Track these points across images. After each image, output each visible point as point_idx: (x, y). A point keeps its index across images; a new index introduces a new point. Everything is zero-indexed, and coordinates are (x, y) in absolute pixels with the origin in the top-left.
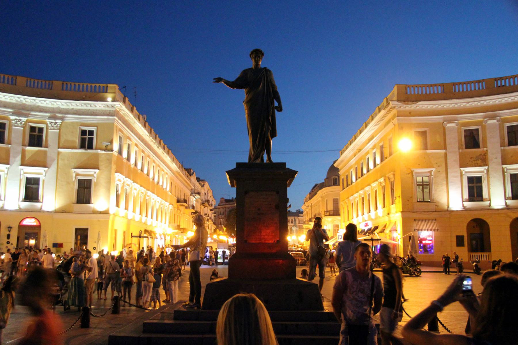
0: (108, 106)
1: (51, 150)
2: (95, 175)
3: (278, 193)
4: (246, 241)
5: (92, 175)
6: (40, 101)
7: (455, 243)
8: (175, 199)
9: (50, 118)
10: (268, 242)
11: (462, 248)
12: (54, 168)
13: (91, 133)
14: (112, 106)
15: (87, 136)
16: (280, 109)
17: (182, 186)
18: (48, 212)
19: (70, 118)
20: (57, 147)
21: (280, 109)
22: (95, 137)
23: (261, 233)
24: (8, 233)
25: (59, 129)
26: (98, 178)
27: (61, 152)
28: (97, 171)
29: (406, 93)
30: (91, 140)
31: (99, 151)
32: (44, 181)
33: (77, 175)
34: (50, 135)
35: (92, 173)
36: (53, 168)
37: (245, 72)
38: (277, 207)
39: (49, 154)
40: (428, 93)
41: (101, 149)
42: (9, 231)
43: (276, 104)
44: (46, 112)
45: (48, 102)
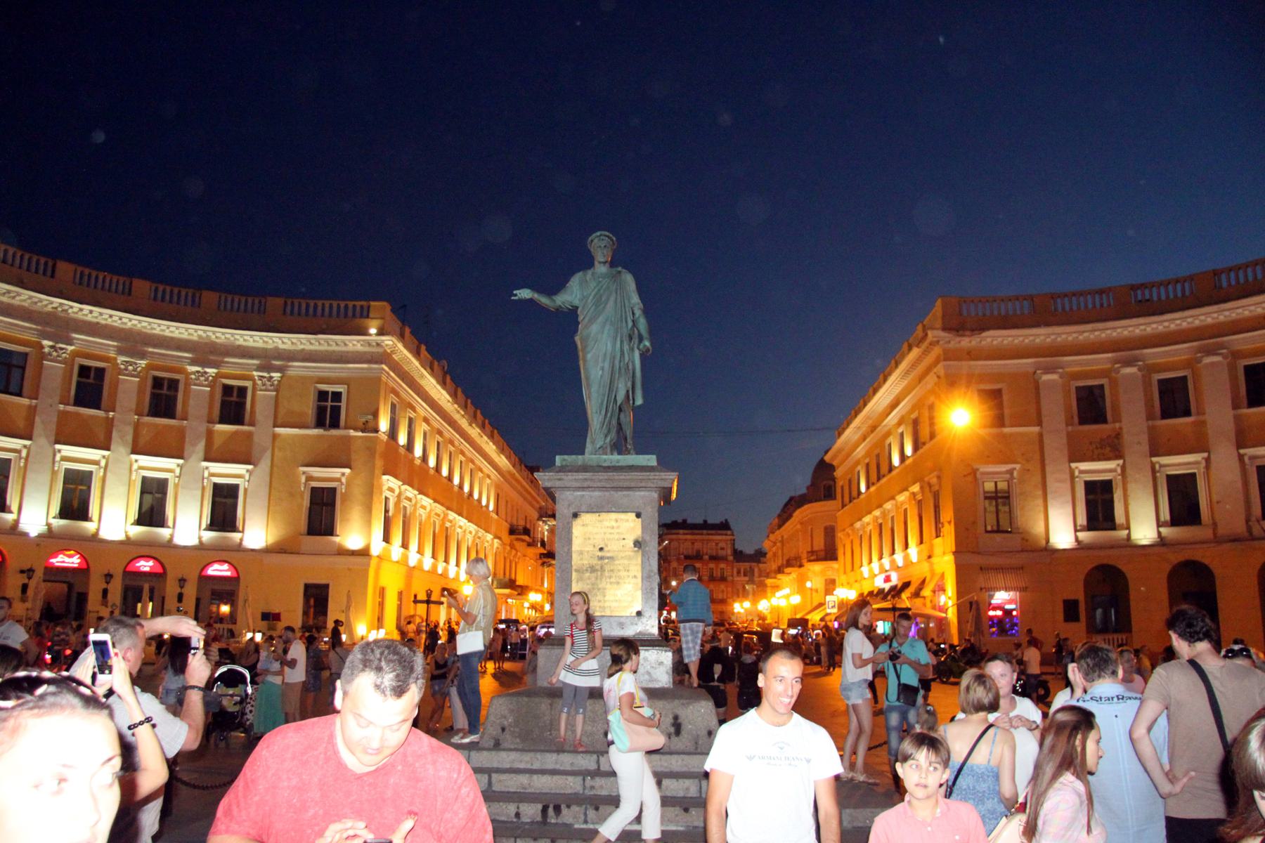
0: (370, 345)
1: (260, 430)
2: (344, 480)
3: (638, 516)
5: (338, 480)
6: (242, 336)
7: (1060, 616)
8: (506, 526)
9: (259, 368)
11: (1072, 626)
12: (265, 464)
13: (337, 396)
14: (378, 345)
15: (329, 404)
17: (520, 500)
18: (253, 550)
19: (298, 369)
20: (271, 423)
22: (343, 405)
24: (104, 586)
25: (277, 390)
26: (348, 485)
27: (279, 435)
28: (347, 471)
30: (336, 411)
31: (352, 433)
32: (246, 490)
33: (310, 478)
34: (260, 402)
35: (338, 475)
36: (265, 464)
39: (256, 439)
41: (355, 429)
42: (108, 583)
44: (252, 357)
45: (257, 338)
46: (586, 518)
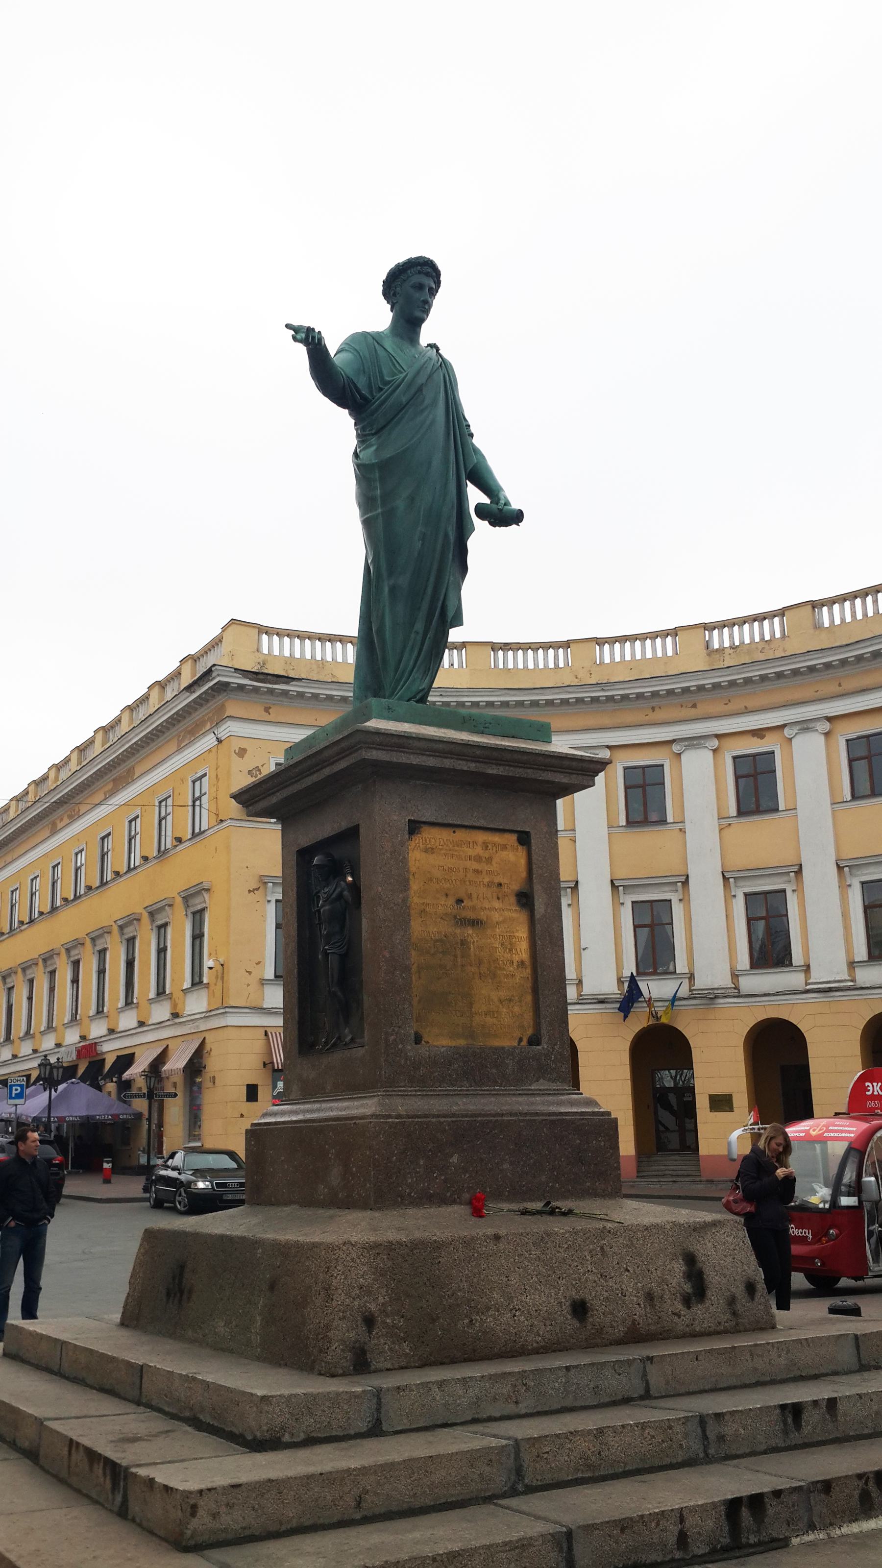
3: (524, 839)
4: (418, 1039)
10: (497, 1043)
16: (503, 516)
21: (503, 516)
23: (471, 1005)
37: (364, 344)
38: (525, 899)
43: (475, 496)
46: (431, 836)
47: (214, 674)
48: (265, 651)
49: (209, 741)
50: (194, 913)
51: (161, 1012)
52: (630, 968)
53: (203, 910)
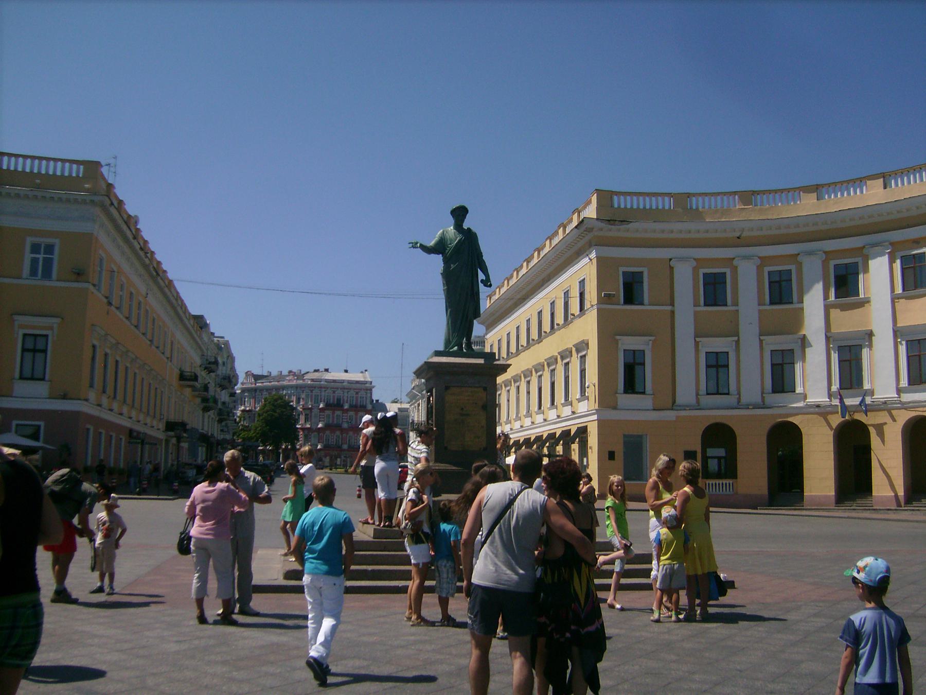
3: (485, 389)
4: (446, 448)
16: (487, 283)
22: (56, 257)
29: (612, 206)
30: (48, 263)
38: (484, 407)
40: (648, 207)
47: (585, 221)
48: (616, 206)
49: (586, 260)
50: (581, 357)
51: (567, 411)
52: (835, 387)
53: (585, 356)
